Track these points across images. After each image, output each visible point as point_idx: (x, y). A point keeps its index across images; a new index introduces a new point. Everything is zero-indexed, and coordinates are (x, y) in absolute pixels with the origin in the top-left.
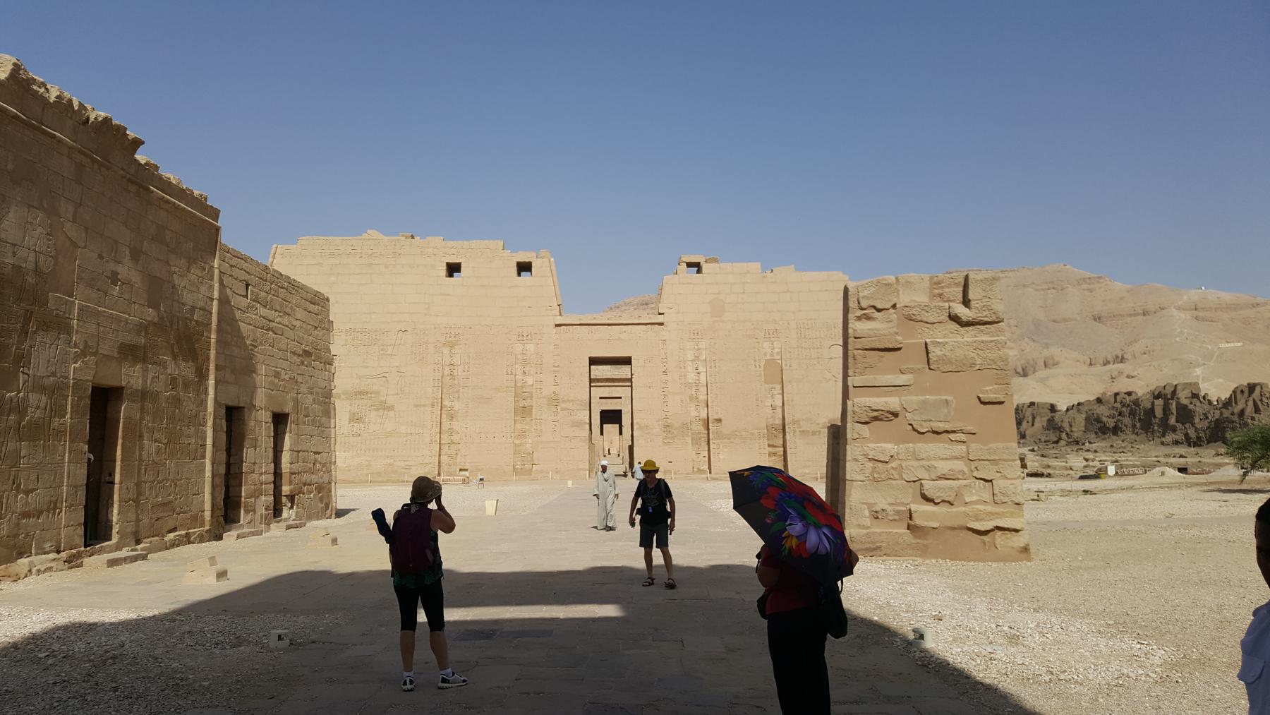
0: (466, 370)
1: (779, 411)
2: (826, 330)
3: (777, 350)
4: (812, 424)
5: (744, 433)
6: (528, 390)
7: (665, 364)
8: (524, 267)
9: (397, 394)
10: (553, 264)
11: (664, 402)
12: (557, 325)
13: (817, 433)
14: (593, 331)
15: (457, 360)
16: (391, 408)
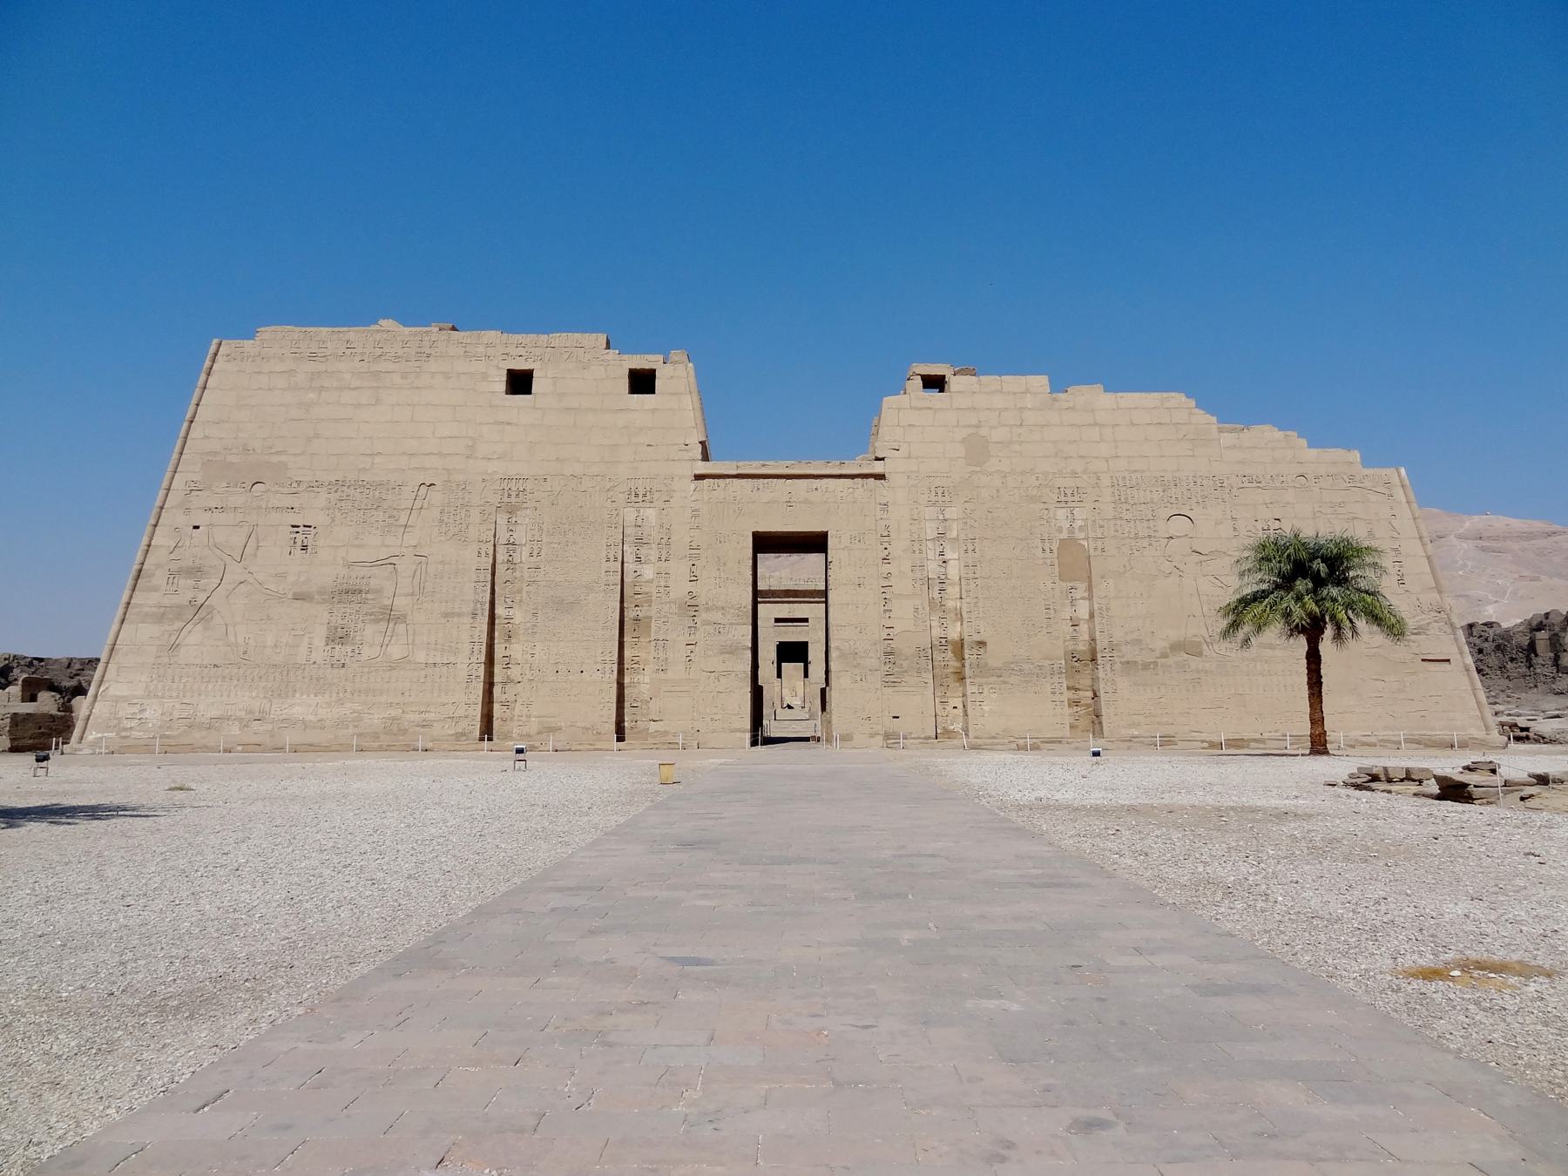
0: (535, 554)
1: (1084, 627)
2: (1160, 489)
3: (1079, 523)
4: (1142, 649)
5: (1025, 666)
6: (647, 590)
7: (886, 545)
8: (642, 382)
9: (412, 594)
10: (692, 373)
11: (885, 611)
12: (699, 477)
13: (1152, 666)
14: (761, 487)
15: (520, 536)
16: (401, 619)
